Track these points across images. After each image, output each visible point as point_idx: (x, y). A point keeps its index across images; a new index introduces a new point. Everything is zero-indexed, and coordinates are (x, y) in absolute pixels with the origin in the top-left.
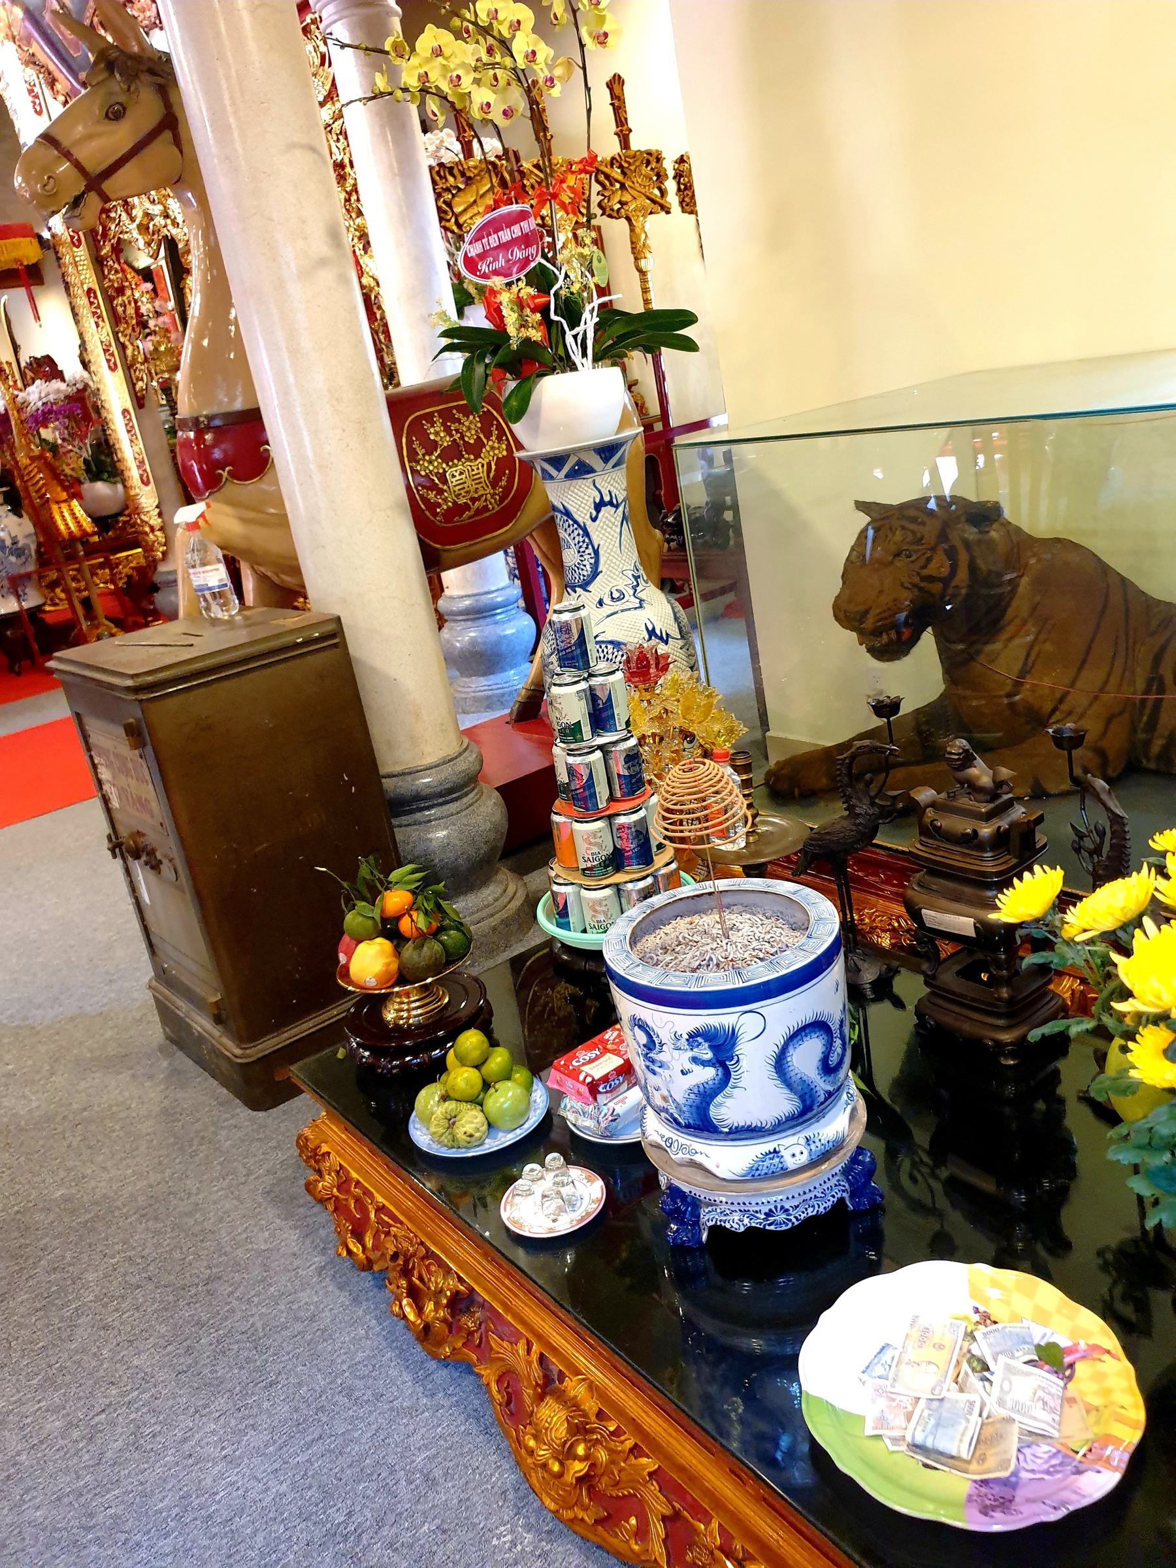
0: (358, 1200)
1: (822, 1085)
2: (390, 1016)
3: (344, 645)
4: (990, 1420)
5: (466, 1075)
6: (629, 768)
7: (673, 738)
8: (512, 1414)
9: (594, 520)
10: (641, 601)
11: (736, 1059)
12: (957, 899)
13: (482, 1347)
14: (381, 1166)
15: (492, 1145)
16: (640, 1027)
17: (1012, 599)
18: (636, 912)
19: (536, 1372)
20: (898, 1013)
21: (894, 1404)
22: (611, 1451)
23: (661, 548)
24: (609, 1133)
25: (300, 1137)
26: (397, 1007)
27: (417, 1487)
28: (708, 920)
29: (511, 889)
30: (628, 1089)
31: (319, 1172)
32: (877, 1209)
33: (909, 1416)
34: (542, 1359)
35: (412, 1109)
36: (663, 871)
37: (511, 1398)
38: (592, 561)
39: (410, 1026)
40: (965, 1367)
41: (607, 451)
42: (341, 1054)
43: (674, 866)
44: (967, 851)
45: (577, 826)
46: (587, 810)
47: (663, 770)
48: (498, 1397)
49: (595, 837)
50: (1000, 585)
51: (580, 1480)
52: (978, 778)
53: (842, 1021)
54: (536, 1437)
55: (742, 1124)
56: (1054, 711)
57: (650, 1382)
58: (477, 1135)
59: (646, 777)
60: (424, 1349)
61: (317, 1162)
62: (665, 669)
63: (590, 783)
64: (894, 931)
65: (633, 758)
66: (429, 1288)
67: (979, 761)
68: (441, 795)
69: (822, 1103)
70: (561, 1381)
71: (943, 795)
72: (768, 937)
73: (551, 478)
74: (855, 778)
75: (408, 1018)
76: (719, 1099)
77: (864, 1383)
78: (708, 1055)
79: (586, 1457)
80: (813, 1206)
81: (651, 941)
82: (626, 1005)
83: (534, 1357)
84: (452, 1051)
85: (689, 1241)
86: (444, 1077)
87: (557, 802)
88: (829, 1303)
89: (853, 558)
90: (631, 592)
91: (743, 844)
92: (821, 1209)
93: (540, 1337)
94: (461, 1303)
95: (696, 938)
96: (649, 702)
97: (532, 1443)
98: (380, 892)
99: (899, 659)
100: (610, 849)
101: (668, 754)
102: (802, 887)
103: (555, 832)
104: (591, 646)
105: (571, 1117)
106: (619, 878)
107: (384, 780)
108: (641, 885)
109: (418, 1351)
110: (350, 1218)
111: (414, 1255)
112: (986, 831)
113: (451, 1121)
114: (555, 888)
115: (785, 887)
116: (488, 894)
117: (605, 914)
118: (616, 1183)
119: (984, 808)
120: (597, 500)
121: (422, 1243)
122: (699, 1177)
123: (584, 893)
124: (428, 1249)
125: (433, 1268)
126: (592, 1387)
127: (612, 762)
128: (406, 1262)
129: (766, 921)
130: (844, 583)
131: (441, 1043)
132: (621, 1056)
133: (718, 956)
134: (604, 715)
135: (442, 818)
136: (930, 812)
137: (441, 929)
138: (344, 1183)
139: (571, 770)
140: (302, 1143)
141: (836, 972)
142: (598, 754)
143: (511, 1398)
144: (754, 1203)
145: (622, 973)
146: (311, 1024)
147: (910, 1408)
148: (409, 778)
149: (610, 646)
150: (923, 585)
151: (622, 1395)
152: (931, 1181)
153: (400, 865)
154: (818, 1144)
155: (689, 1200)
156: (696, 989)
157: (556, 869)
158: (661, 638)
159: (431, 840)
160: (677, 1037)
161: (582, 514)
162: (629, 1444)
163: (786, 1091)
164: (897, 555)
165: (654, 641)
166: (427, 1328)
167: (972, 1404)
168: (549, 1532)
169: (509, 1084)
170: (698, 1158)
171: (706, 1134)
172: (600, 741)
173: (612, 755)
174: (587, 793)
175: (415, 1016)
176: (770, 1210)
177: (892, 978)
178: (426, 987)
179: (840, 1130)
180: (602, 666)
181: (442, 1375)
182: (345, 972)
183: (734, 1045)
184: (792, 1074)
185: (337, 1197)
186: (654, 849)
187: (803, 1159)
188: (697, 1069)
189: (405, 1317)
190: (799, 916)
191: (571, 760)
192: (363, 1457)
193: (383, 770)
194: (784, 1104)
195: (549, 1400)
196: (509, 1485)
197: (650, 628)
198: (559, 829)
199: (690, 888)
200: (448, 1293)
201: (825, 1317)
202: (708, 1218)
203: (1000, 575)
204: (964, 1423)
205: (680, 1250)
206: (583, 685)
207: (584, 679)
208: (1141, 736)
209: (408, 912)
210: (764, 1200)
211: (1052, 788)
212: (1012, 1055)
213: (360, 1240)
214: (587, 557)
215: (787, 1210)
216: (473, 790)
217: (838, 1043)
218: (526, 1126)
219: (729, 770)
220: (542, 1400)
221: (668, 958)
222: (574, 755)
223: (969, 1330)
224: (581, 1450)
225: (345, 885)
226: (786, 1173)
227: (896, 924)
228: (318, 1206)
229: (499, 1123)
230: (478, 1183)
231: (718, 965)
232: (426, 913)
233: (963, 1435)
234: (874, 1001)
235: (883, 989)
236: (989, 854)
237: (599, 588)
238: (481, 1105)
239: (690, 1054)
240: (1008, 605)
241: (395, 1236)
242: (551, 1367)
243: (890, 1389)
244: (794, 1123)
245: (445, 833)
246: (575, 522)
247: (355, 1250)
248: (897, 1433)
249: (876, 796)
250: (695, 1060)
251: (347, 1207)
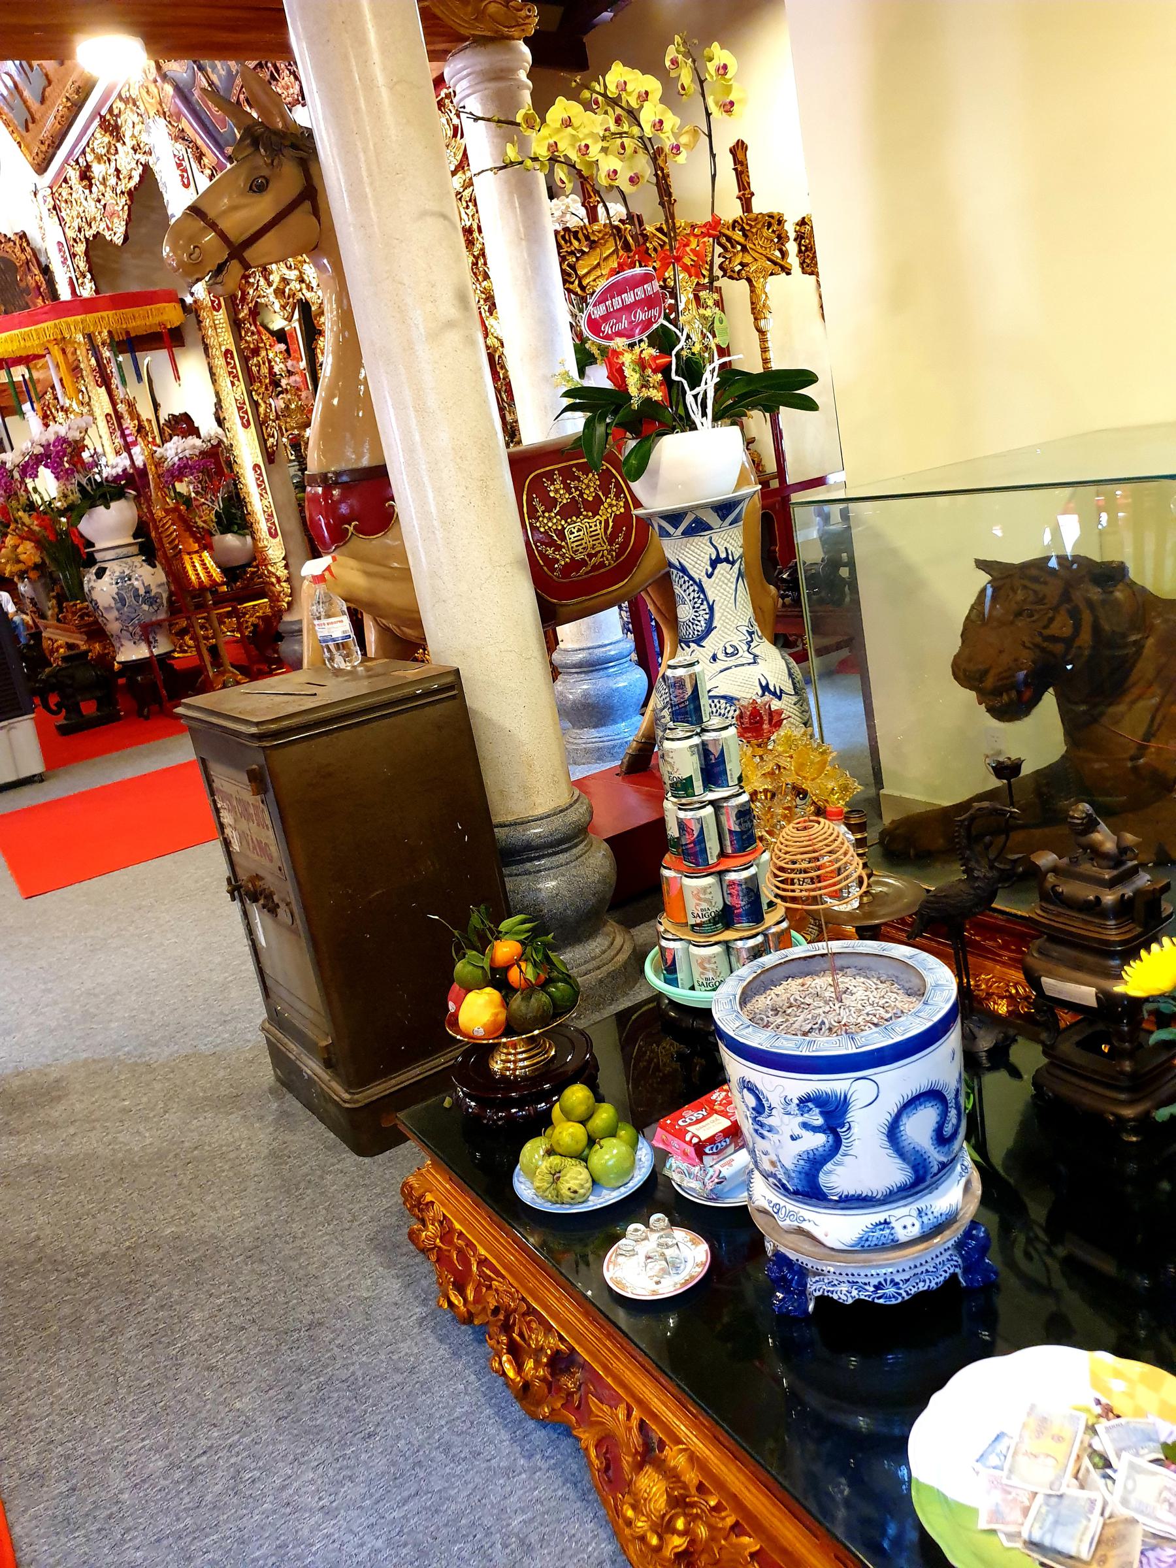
0: (460, 1251)
1: (936, 1156)
2: (497, 1066)
3: (461, 696)
4: (1113, 1520)
5: (571, 1130)
6: (740, 824)
7: (786, 795)
8: (610, 1481)
9: (710, 576)
10: (755, 656)
11: (847, 1126)
13: (581, 1410)
14: (484, 1219)
15: (596, 1202)
16: (749, 1090)
18: (747, 972)
19: (635, 1438)
20: (1015, 1083)
21: (1010, 1497)
22: (711, 1527)
23: (775, 604)
24: (715, 1195)
25: (405, 1184)
26: (503, 1057)
27: (513, 1552)
28: (821, 983)
29: (619, 941)
30: (736, 1151)
31: (423, 1221)
32: (991, 1287)
33: (1026, 1511)
34: (642, 1425)
35: (517, 1162)
36: (773, 930)
37: (610, 1465)
38: (707, 617)
39: (516, 1076)
40: (1086, 1462)
41: (724, 509)
42: (447, 1103)
43: (785, 925)
45: (687, 881)
46: (698, 865)
47: (774, 826)
48: (596, 1462)
49: (705, 893)
50: (1125, 646)
51: (679, 1556)
52: (1102, 843)
53: (957, 1091)
54: (634, 1507)
55: (852, 1192)
57: (753, 1457)
58: (582, 1191)
59: (759, 833)
60: (523, 1407)
61: (421, 1210)
62: (779, 724)
63: (701, 839)
64: (1011, 999)
65: (744, 814)
66: (529, 1345)
67: (1103, 826)
68: (551, 845)
69: (936, 1174)
70: (661, 1450)
71: (1065, 860)
72: (882, 1002)
73: (669, 535)
74: (973, 839)
75: (515, 1069)
76: (829, 1166)
77: (977, 1473)
78: (819, 1121)
79: (684, 1533)
80: (924, 1281)
81: (761, 1002)
82: (736, 1067)
83: (634, 1423)
84: (557, 1105)
85: (795, 1310)
86: (549, 1131)
87: (667, 856)
88: (940, 1383)
89: (973, 617)
90: (746, 648)
91: (856, 904)
92: (933, 1285)
93: (641, 1403)
94: (561, 1362)
95: (808, 1000)
96: (761, 757)
97: (630, 1513)
98: (490, 942)
99: (1019, 719)
100: (720, 906)
101: (780, 811)
102: (917, 951)
103: (665, 887)
104: (704, 701)
105: (676, 1177)
106: (728, 935)
107: (496, 830)
108: (751, 943)
109: (516, 1410)
110: (453, 1270)
111: (515, 1310)
112: (1109, 898)
113: (556, 1176)
114: (664, 943)
115: (901, 951)
116: (595, 946)
117: (714, 971)
118: (721, 1246)
120: (714, 557)
121: (523, 1299)
122: (806, 1246)
123: (693, 949)
124: (529, 1305)
125: (534, 1325)
126: (693, 1459)
127: (723, 818)
128: (507, 1318)
129: (881, 986)
130: (963, 642)
131: (546, 1097)
132: (728, 1118)
133: (831, 1019)
134: (717, 770)
135: (552, 868)
136: (1051, 878)
137: (550, 981)
138: (447, 1233)
139: (682, 825)
140: (406, 1191)
141: (953, 1040)
142: (710, 809)
143: (610, 1465)
144: (863, 1274)
145: (732, 1034)
146: (418, 1071)
147: (1027, 1503)
148: (520, 828)
149: (722, 701)
150: (1045, 644)
151: (723, 1468)
152: (1049, 1261)
153: (510, 916)
154: (931, 1216)
155: (795, 1268)
156: (808, 1054)
157: (664, 924)
158: (774, 694)
159: (540, 890)
160: (787, 1102)
161: (698, 570)
162: (730, 1521)
163: (899, 1161)
164: (1019, 614)
165: (768, 696)
166: (527, 1386)
167: (1093, 1502)
169: (614, 1140)
170: (806, 1226)
171: (814, 1201)
172: (711, 796)
173: (724, 811)
174: (698, 848)
175: (522, 1068)
176: (880, 1283)
177: (1009, 1046)
178: (532, 1039)
179: (954, 1203)
180: (715, 722)
181: (540, 1436)
182: (454, 1021)
183: (845, 1112)
184: (906, 1143)
185: (439, 1248)
186: (765, 907)
187: (915, 1231)
188: (807, 1135)
189: (504, 1374)
190: (916, 981)
191: (682, 814)
192: (460, 1515)
193: (496, 820)
194: (896, 1173)
195: (648, 1469)
196: (605, 1556)
197: (764, 684)
198: (668, 885)
199: (801, 948)
200: (549, 1352)
201: (936, 1399)
202: (815, 1287)
203: (1124, 636)
204: (1084, 1522)
205: (785, 1321)
206: (696, 740)
207: (697, 734)
209: (517, 962)
210: (873, 1272)
213: (461, 1291)
214: (702, 613)
215: (897, 1284)
216: (582, 841)
217: (953, 1113)
218: (630, 1185)
219: (843, 829)
220: (641, 1468)
221: (779, 1020)
222: (685, 810)
223: (1090, 1423)
224: (680, 1524)
225: (456, 933)
226: (897, 1245)
227: (1014, 991)
228: (422, 1255)
229: (603, 1181)
230: (581, 1240)
231: (830, 1029)
232: (535, 965)
233: (1083, 1534)
234: (989, 1069)
235: (999, 1058)
236: (1113, 922)
237: (712, 643)
238: (586, 1160)
239: (801, 1119)
240: (1133, 665)
241: (496, 1290)
242: (653, 1434)
243: (1005, 1481)
244: (905, 1194)
245: (554, 883)
246: (691, 578)
247: (456, 1302)
248: (1012, 1529)
249: (995, 860)
250: (805, 1126)
251: (450, 1258)
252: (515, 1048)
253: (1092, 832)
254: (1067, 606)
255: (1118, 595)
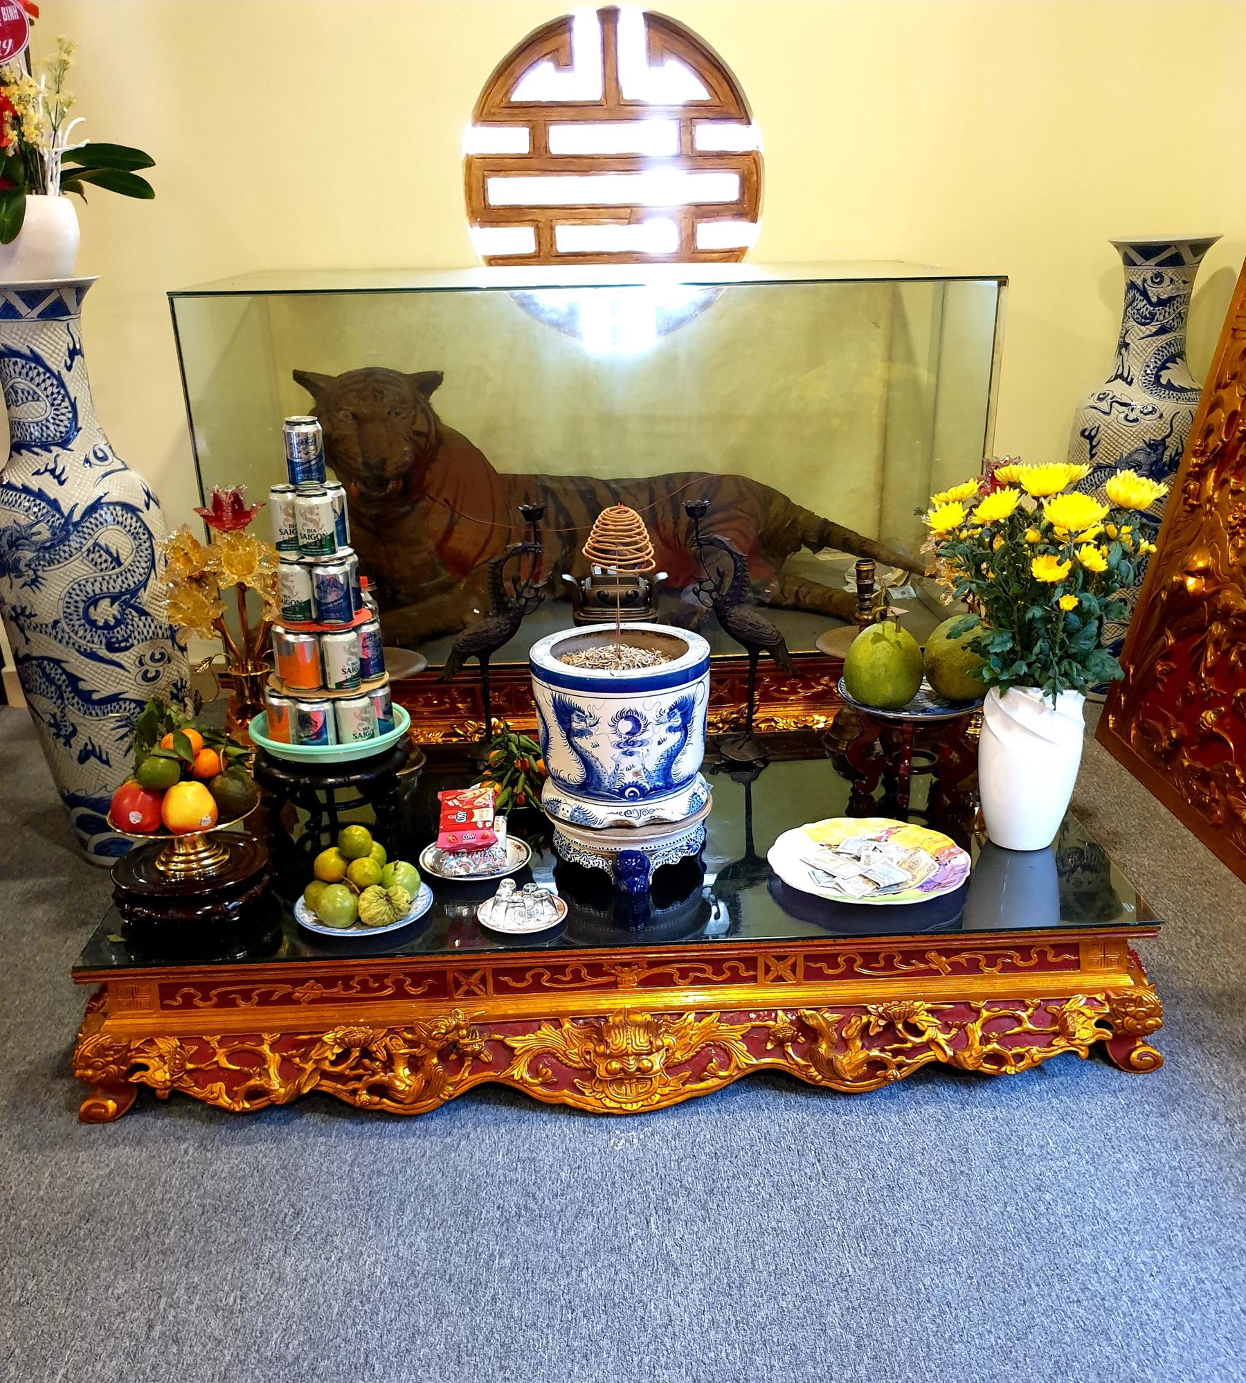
38: (70, 415)
76: (679, 756)
168: (641, 1123)
170: (656, 814)
202: (655, 864)
239: (668, 725)
246: (48, 369)
252: (195, 847)
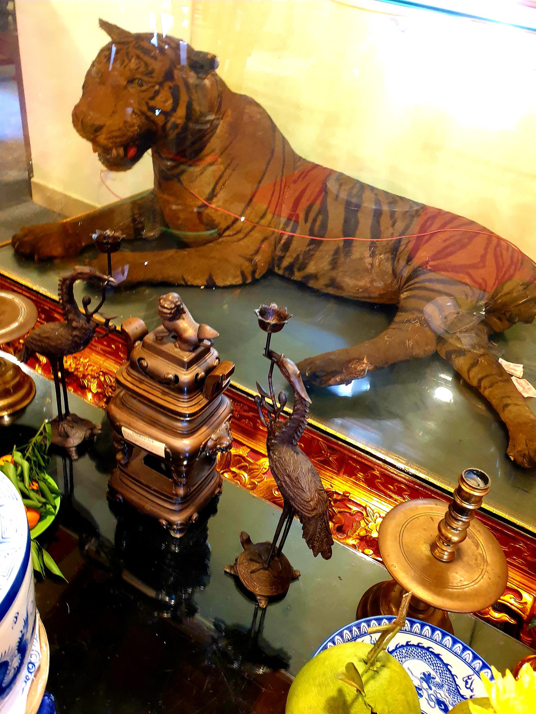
12: (154, 423)
17: (211, 137)
44: (167, 390)
52: (185, 330)
56: (228, 228)
67: (188, 315)
119: (187, 357)
130: (83, 95)
164: (131, 81)
208: (279, 253)
211: (220, 282)
212: (180, 531)
236: (186, 397)
253: (179, 319)
254: (171, 84)
255: (207, 82)
